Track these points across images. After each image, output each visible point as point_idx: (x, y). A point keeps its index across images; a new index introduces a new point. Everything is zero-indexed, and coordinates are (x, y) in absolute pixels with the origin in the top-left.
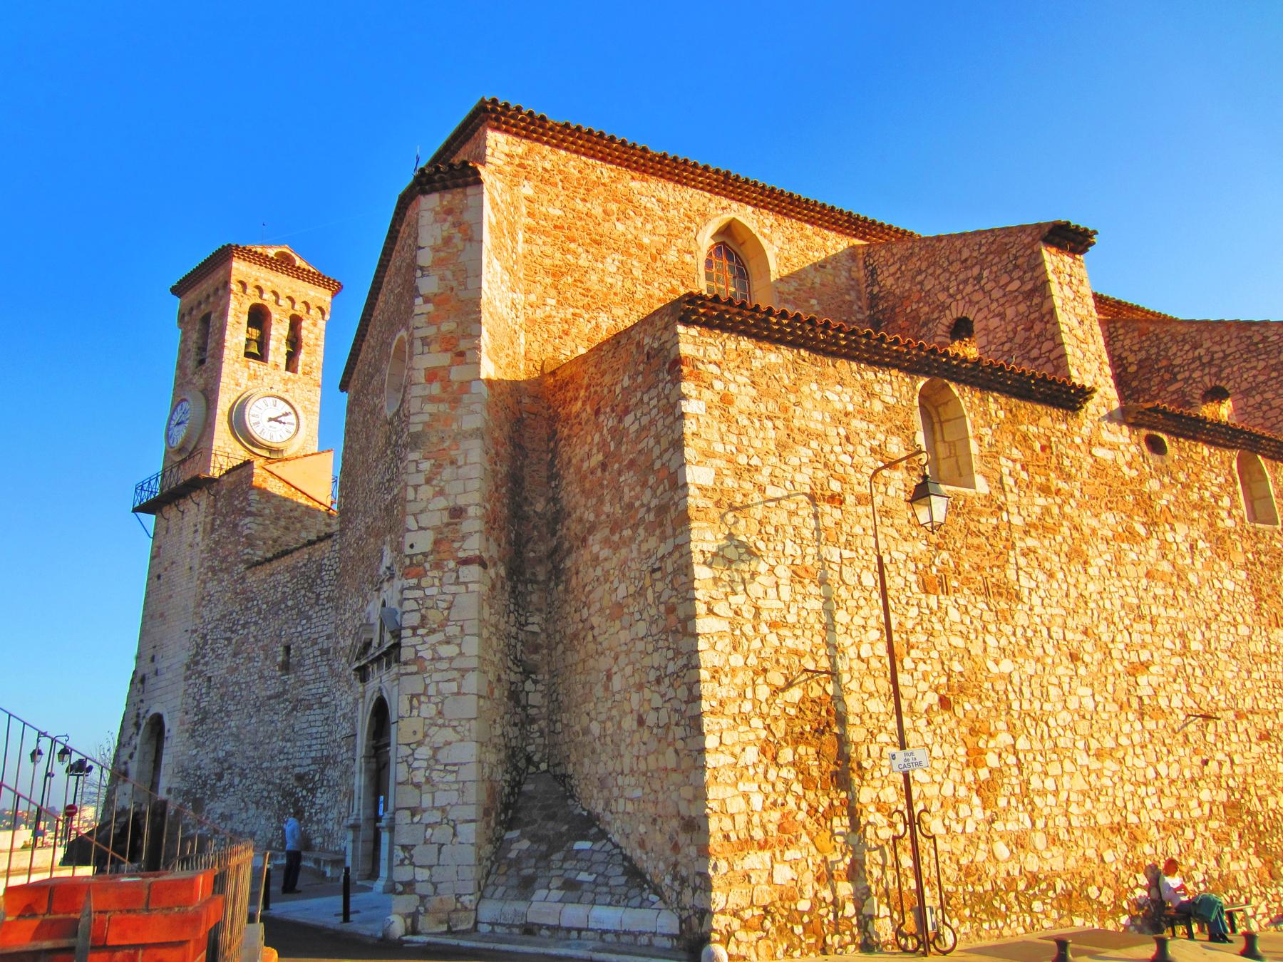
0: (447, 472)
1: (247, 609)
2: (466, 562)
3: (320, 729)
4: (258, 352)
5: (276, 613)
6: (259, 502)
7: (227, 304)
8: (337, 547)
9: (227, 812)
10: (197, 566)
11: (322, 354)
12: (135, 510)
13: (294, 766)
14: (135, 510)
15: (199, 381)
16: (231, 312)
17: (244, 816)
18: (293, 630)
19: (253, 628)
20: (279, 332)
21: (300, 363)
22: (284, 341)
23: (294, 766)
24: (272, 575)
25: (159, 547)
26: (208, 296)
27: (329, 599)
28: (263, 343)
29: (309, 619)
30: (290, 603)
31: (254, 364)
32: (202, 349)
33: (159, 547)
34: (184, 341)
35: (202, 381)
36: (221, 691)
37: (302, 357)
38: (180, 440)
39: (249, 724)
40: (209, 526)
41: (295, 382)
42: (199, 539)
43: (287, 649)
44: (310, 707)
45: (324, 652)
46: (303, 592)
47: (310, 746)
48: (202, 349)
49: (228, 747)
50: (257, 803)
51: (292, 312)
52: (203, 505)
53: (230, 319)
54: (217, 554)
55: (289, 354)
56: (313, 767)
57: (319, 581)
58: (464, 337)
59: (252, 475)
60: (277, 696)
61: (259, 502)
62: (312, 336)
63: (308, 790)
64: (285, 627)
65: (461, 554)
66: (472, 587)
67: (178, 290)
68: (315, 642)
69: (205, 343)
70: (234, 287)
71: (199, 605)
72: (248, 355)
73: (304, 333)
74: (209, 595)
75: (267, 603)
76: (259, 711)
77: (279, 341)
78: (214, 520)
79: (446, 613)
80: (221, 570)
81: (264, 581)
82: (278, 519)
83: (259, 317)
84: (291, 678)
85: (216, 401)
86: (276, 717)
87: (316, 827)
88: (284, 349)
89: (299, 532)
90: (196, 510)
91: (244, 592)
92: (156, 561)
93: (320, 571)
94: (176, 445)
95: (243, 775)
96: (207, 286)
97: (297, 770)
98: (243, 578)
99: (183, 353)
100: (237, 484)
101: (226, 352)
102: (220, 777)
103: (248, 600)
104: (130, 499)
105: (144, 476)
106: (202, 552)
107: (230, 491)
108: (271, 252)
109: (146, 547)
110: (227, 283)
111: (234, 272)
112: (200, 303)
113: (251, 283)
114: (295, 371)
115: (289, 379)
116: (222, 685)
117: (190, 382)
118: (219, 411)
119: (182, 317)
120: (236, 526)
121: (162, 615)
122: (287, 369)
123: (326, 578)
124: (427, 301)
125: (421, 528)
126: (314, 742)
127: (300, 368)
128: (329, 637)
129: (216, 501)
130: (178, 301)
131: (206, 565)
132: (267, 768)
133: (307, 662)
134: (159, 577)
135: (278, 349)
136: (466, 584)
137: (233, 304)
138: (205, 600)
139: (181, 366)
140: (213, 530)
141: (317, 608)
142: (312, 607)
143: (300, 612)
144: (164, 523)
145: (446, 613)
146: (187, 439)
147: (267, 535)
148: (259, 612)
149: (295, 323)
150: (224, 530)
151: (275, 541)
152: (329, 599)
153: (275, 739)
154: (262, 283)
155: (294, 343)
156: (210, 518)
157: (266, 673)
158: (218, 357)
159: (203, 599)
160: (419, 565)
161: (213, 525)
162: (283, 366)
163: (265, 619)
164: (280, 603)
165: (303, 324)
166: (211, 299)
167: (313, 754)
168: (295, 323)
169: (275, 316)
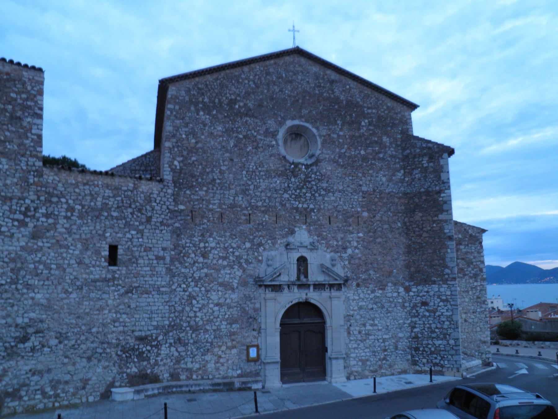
3: (160, 308)
9: (40, 367)
13: (133, 331)
17: (70, 368)
18: (120, 235)
19: (62, 221)
23: (133, 331)
30: (115, 214)
36: (12, 265)
39: (68, 298)
43: (113, 249)
44: (148, 293)
45: (158, 258)
46: (130, 210)
47: (150, 318)
49: (32, 315)
50: (89, 359)
56: (155, 331)
57: (148, 207)
60: (105, 280)
63: (152, 346)
64: (109, 230)
68: (148, 249)
75: (83, 207)
76: (82, 289)
81: (76, 185)
84: (120, 270)
86: (105, 296)
87: (163, 368)
95: (61, 337)
97: (137, 334)
102: (24, 339)
103: (51, 195)
116: (13, 260)
126: (156, 316)
128: (164, 249)
132: (98, 333)
133: (141, 261)
141: (149, 226)
143: (127, 224)
152: (162, 223)
153: (106, 312)
157: (87, 261)
163: (80, 217)
164: (102, 210)
167: (155, 323)
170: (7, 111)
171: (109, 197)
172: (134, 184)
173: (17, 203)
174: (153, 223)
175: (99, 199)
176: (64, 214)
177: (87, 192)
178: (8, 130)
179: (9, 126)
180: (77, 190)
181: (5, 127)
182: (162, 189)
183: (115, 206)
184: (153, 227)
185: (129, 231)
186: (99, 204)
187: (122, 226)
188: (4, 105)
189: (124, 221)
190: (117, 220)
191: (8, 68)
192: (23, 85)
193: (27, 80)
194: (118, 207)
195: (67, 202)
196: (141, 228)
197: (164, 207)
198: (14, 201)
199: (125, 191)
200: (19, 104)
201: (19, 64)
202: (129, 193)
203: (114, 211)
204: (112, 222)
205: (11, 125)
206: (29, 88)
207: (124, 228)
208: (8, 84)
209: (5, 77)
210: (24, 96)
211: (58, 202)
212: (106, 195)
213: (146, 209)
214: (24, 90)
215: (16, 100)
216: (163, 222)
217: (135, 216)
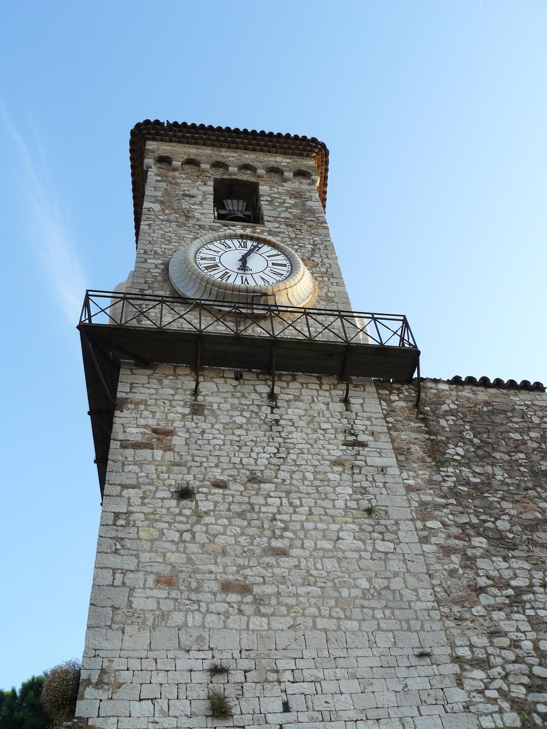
40: (417, 450)
74: (501, 584)
106: (409, 489)
170: (521, 465)
179: (539, 490)
181: (531, 493)
188: (510, 456)
191: (483, 395)
192: (523, 418)
193: (524, 408)
200: (534, 449)
201: (498, 383)
205: (542, 488)
206: (536, 420)
208: (498, 419)
209: (485, 409)
210: (533, 434)
214: (531, 425)
215: (525, 443)
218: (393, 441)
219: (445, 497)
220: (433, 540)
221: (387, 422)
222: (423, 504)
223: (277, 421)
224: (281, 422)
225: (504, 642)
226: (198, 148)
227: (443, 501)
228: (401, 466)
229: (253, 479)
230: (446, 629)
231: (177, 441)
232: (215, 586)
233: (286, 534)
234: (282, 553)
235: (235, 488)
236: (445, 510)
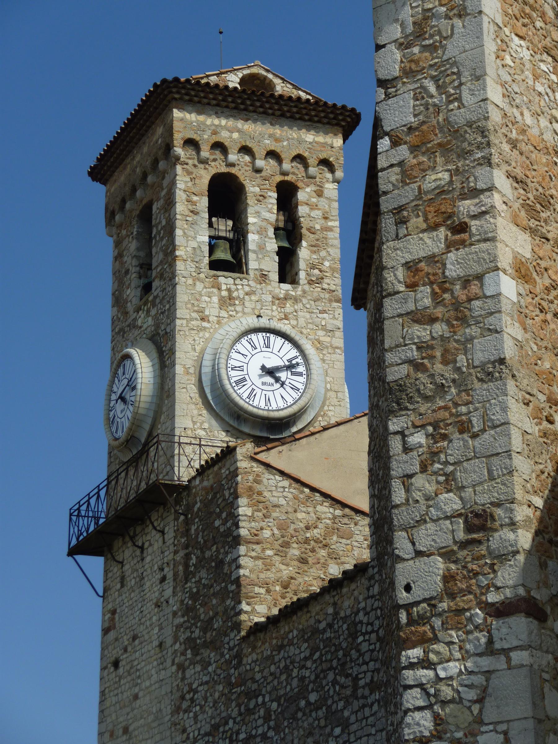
0: (457, 447)
1: (250, 711)
2: (500, 611)
4: (230, 259)
5: (294, 718)
6: (252, 518)
7: (173, 183)
8: (376, 589)
10: (169, 641)
11: (337, 242)
12: (72, 552)
14: (72, 552)
15: (146, 322)
16: (180, 196)
20: (261, 215)
21: (302, 265)
22: (271, 232)
24: (281, 648)
25: (114, 612)
26: (145, 176)
27: (373, 686)
28: (238, 243)
29: (345, 725)
31: (226, 280)
32: (146, 266)
33: (114, 612)
34: (119, 257)
35: (150, 321)
37: (304, 253)
38: (127, 424)
41: (296, 300)
42: (169, 592)
48: (146, 266)
51: (279, 178)
52: (170, 534)
53: (180, 208)
54: (197, 617)
55: (281, 252)
58: (463, 197)
59: (235, 473)
61: (252, 518)
62: (316, 213)
65: (492, 597)
66: (517, 657)
67: (100, 172)
69: (149, 255)
70: (179, 150)
71: (177, 710)
72: (216, 265)
73: (302, 210)
75: (278, 699)
77: (261, 232)
78: (187, 557)
79: (476, 709)
80: (205, 645)
81: (270, 658)
82: (286, 545)
83: (226, 197)
85: (172, 351)
88: (272, 245)
89: (325, 566)
90: (160, 545)
91: (242, 682)
92: (112, 635)
93: (354, 635)
94: (121, 434)
96: (140, 158)
98: (239, 656)
99: (120, 276)
100: (216, 490)
101: (180, 266)
104: (61, 536)
105: (79, 494)
106: (175, 614)
107: (206, 504)
108: (233, 80)
109: (93, 612)
110: (168, 147)
111: (177, 125)
112: (134, 190)
113: (206, 139)
114: (294, 282)
115: (287, 298)
117: (133, 326)
118: (179, 369)
119: (110, 216)
120: (220, 563)
121: (126, 730)
122: (282, 280)
123: (365, 647)
124: (396, 143)
125: (419, 554)
127: (302, 275)
129: (187, 523)
130: (99, 189)
131: (182, 638)
134: (116, 664)
135: (261, 247)
136: (505, 652)
137: (182, 183)
138: (185, 700)
139: (118, 301)
140: (187, 577)
141: (356, 705)
142: (348, 703)
144: (116, 569)
145: (476, 709)
146: (136, 423)
147: (271, 575)
148: (267, 718)
149: (287, 195)
150: (203, 574)
151: (285, 586)
152: (373, 686)
154: (224, 136)
155: (290, 233)
156: (182, 553)
158: (170, 277)
159: (183, 698)
160: (423, 619)
161: (186, 566)
162: (275, 276)
163: (277, 729)
165: (301, 196)
166: (150, 179)
168: (287, 195)
169: (252, 189)
171: (306, 659)
172: (335, 604)
173: (223, 732)
174: (360, 692)
175: (295, 673)
176: (260, 731)
177: (282, 665)
178: (214, 595)
180: (273, 668)
182: (368, 589)
183: (313, 677)
184: (362, 701)
185: (332, 730)
186: (295, 683)
187: (323, 723)
189: (324, 708)
190: (317, 709)
194: (317, 677)
195: (264, 703)
196: (346, 714)
197: (374, 636)
198: (221, 729)
199: (324, 630)
202: (328, 635)
203: (313, 691)
204: (310, 720)
207: (326, 726)
210: (224, 515)
211: (255, 707)
212: (302, 656)
213: (351, 661)
216: (372, 681)
217: (337, 688)
218: (174, 565)
219: (183, 616)
220: (176, 661)
221: (175, 546)
222: (177, 627)
223: (142, 574)
224: (145, 574)
225: (185, 735)
226: (125, 168)
227: (182, 620)
228: (174, 593)
229: (134, 638)
230: (171, 733)
231: (117, 616)
232: (121, 731)
233: (139, 681)
234: (136, 697)
235: (129, 649)
236: (182, 630)
